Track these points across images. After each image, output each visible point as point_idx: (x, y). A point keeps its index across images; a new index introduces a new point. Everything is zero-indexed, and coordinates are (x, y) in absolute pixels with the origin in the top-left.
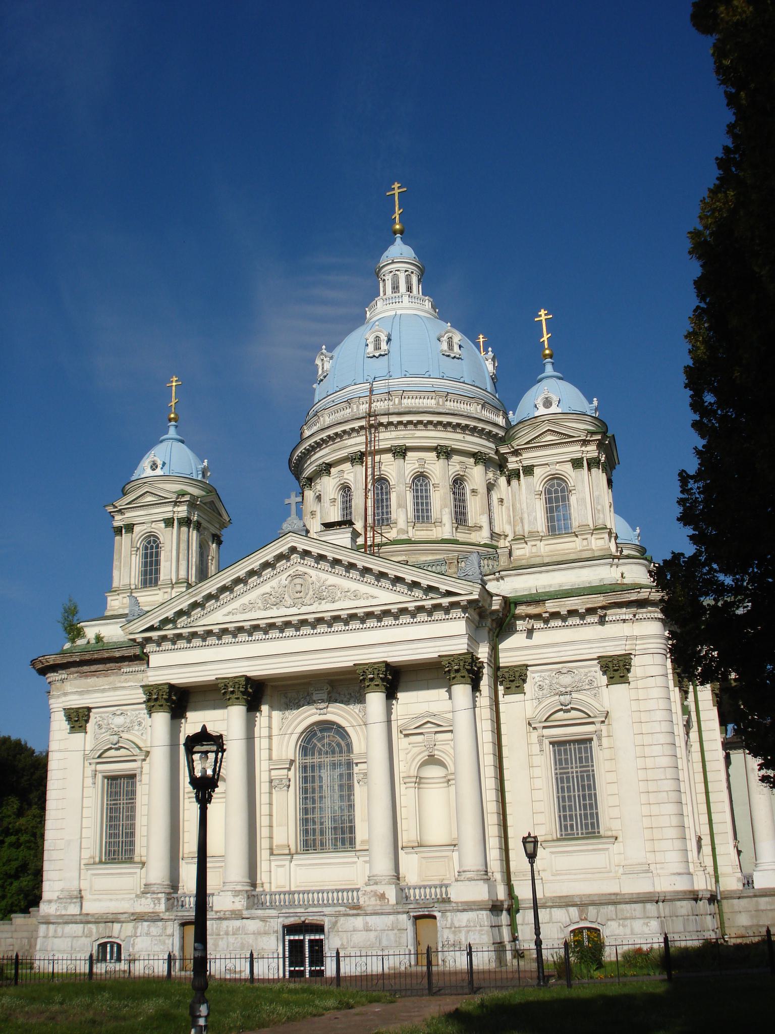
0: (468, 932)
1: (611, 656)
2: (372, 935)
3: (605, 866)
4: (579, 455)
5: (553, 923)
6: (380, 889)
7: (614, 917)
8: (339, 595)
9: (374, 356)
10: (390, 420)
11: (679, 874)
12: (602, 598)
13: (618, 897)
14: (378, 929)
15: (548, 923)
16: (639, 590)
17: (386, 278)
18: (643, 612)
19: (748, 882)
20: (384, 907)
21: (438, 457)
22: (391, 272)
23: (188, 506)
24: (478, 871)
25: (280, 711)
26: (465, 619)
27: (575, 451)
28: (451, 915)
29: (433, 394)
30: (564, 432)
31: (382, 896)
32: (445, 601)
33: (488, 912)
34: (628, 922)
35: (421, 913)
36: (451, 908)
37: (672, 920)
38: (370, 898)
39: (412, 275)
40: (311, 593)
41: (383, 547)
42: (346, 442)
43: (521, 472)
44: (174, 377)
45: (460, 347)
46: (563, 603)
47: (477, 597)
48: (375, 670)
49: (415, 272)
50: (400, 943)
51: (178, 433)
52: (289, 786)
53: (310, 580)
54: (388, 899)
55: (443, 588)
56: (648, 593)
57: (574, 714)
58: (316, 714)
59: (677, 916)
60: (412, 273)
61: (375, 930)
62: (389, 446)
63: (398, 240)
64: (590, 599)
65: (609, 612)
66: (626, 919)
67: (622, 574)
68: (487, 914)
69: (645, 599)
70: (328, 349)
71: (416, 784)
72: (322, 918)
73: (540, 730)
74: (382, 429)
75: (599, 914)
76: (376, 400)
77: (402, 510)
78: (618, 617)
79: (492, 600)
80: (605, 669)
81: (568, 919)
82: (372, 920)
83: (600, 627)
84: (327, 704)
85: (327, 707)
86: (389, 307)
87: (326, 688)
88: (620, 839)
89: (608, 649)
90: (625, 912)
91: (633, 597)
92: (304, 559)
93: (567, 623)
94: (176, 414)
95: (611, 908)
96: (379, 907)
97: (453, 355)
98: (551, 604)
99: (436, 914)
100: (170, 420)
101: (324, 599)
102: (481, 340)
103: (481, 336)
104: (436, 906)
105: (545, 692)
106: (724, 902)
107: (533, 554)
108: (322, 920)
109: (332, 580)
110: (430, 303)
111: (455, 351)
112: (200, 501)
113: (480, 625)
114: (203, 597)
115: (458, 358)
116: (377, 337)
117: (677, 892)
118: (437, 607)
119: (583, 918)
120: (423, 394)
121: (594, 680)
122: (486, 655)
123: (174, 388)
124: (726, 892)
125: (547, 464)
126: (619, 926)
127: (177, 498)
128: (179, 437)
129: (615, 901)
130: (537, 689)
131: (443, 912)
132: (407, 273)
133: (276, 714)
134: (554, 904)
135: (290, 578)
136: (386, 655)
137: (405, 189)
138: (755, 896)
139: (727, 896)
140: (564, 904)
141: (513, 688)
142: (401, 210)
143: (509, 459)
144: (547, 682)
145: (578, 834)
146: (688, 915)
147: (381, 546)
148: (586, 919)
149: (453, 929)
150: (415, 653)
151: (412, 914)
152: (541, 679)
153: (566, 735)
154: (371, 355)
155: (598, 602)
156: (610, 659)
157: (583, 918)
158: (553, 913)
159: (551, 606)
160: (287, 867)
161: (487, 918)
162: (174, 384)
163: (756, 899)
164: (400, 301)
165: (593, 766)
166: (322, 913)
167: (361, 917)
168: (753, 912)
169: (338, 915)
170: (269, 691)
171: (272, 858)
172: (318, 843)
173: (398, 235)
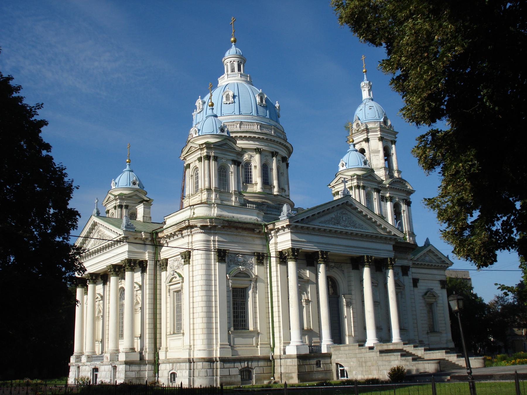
2: (105, 372)
4: (199, 156)
11: (199, 350)
24: (126, 349)
39: (234, 62)
46: (168, 231)
56: (188, 223)
63: (233, 46)
66: (181, 369)
79: (142, 234)
94: (129, 160)
95: (179, 364)
97: (228, 103)
100: (127, 162)
112: (124, 197)
114: (80, 243)
115: (232, 103)
132: (232, 62)
151: (113, 365)
173: (233, 43)
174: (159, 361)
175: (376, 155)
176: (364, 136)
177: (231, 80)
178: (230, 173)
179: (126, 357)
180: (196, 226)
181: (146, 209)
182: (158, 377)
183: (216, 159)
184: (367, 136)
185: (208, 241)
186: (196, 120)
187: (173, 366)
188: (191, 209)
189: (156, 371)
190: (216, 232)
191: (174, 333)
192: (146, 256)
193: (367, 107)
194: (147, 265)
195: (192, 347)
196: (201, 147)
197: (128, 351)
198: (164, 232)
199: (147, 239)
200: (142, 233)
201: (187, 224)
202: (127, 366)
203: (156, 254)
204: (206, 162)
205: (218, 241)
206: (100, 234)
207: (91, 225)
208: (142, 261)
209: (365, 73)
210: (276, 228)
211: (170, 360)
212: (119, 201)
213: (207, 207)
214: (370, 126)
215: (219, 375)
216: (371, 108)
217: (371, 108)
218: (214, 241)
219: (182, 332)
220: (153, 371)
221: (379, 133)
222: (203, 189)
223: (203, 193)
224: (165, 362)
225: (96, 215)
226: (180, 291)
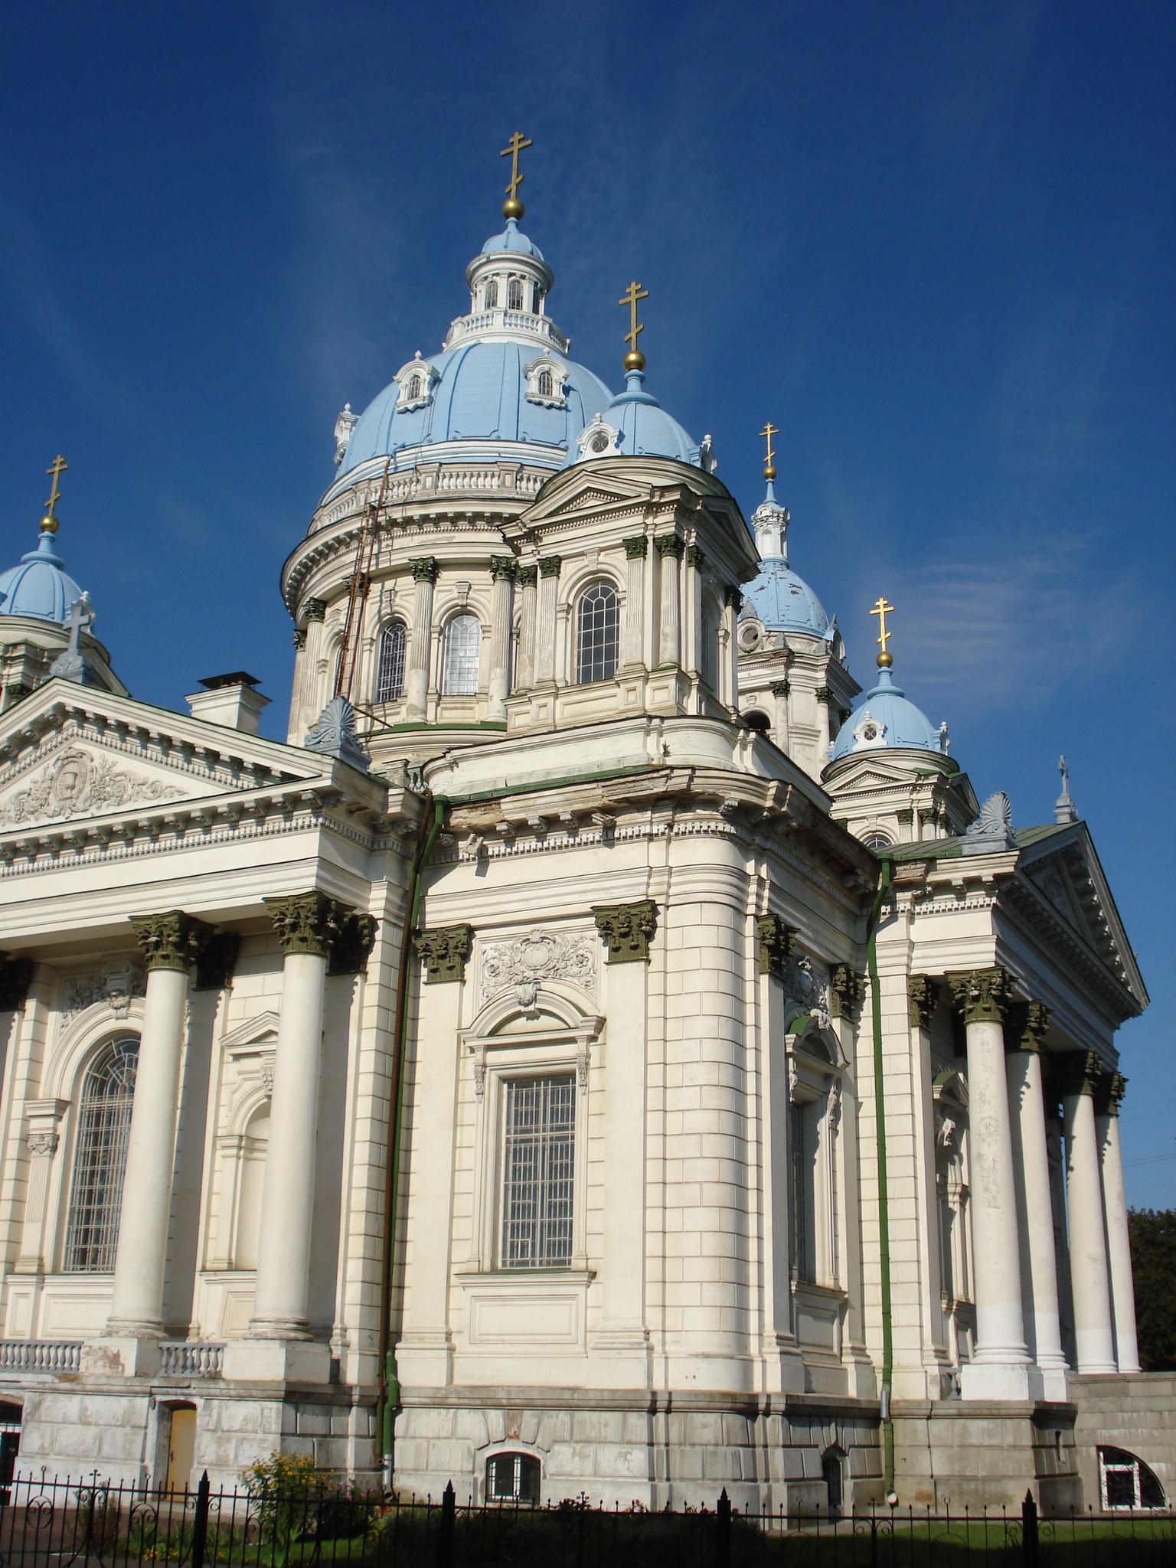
0: (242, 1440)
1: (616, 908)
2: (91, 1432)
3: (567, 1331)
4: (638, 532)
5: (457, 1439)
6: (114, 1345)
7: (567, 1436)
8: (130, 791)
9: (408, 410)
10: (409, 514)
11: (706, 1356)
12: (600, 791)
13: (576, 1396)
14: (101, 1422)
15: (450, 1438)
16: (668, 772)
17: (478, 290)
18: (687, 820)
19: (949, 1385)
20: (112, 1381)
21: (494, 578)
22: (486, 278)
23: (26, 664)
24: (278, 1321)
25: (62, 1010)
26: (319, 828)
27: (631, 524)
28: (220, 1407)
29: (495, 468)
30: (613, 490)
31: (115, 1360)
32: (276, 793)
33: (280, 1405)
34: (590, 1449)
35: (174, 1398)
36: (218, 1392)
37: (682, 1451)
38: (95, 1362)
39: (522, 281)
40: (88, 788)
41: (374, 738)
42: (343, 559)
43: (539, 572)
44: (59, 456)
45: (567, 390)
46: (531, 802)
47: (328, 783)
48: (163, 928)
49: (528, 275)
50: (130, 1454)
51: (53, 551)
52: (54, 1149)
53: (89, 765)
54: (123, 1366)
55: (277, 768)
56: (686, 779)
57: (545, 1021)
58: (109, 1018)
59: (693, 1445)
60: (523, 277)
61: (97, 1425)
62: (406, 561)
63: (512, 227)
64: (579, 794)
65: (620, 820)
66: (588, 1441)
67: (665, 747)
68: (277, 1409)
69: (682, 791)
70: (353, 411)
71: (242, 1153)
72: (21, 1393)
73: (479, 1054)
74: (397, 531)
75: (541, 1428)
76: (395, 483)
77: (416, 673)
78: (636, 830)
79: (386, 797)
80: (606, 930)
81: (484, 1435)
82: (95, 1404)
83: (607, 849)
84: (127, 998)
85: (129, 1004)
86: (470, 334)
87: (124, 969)
88: (599, 1278)
89: (616, 893)
90: (588, 1428)
91: (658, 787)
92: (83, 728)
93: (546, 844)
94: (55, 519)
95: (563, 1416)
96: (104, 1380)
97: (547, 402)
98: (511, 806)
99: (198, 1402)
100: (43, 528)
101: (105, 799)
102: (769, 432)
103: (769, 427)
104: (193, 1386)
105: (499, 978)
106: (898, 1424)
107: (539, 723)
108: (21, 1398)
109: (124, 763)
110: (547, 327)
111: (554, 395)
113: (376, 847)
115: (560, 408)
116: (416, 376)
117: (697, 1394)
118: (266, 807)
119: (512, 1433)
120: (475, 469)
121: (588, 955)
122: (382, 904)
123: (56, 476)
124: (902, 1404)
125: (582, 554)
126: (574, 1454)
127: (6, 652)
128: (53, 557)
129: (571, 1402)
130: (487, 974)
131: (209, 1398)
133: (53, 1017)
134: (462, 1401)
135: (59, 763)
136: (184, 899)
137: (529, 142)
138: (961, 1416)
139: (903, 1412)
140: (478, 1402)
141: (444, 972)
142: (520, 178)
143: (523, 549)
144: (506, 958)
145: (533, 1263)
146: (717, 1445)
147: (371, 736)
148: (517, 1436)
149: (219, 1433)
150: (232, 894)
151: (158, 1398)
152: (495, 954)
153: (526, 1064)
154: (402, 408)
155: (594, 798)
156: (616, 914)
157: (512, 1433)
158: (459, 1419)
159: (511, 810)
160: (32, 1296)
161: (277, 1417)
162: (57, 469)
163: (963, 1421)
164: (490, 322)
165: (573, 1128)
166: (19, 1384)
167: (79, 1397)
168: (955, 1449)
169: (43, 1390)
170: (41, 975)
171: (11, 1279)
172: (90, 1256)
174: (402, 1393)
175: (806, 742)
176: (776, 674)
177: (520, 335)
178: (721, 633)
179: (289, 1365)
180: (711, 802)
181: (247, 715)
182: (393, 1471)
183: (699, 561)
184: (787, 675)
185: (743, 877)
186: (389, 435)
187: (509, 1422)
188: (648, 733)
189: (383, 1440)
190: (768, 845)
191: (494, 1271)
192: (377, 901)
193: (784, 587)
194: (372, 941)
195: (655, 1339)
196: (656, 500)
197: (292, 1335)
198: (503, 806)
199: (397, 821)
200: (391, 791)
201: (679, 782)
202: (287, 1406)
203: (411, 902)
204: (668, 562)
205: (773, 888)
206: (71, 768)
207: (32, 723)
208: (355, 919)
209: (770, 479)
210: (929, 884)
211: (501, 1394)
212: (20, 668)
213: (722, 734)
214: (796, 645)
215: (781, 1474)
216: (794, 589)
217: (794, 589)
218: (761, 882)
219: (577, 1263)
220: (370, 1441)
221: (822, 675)
222: (650, 670)
223: (650, 684)
224: (451, 1401)
225: (79, 679)
226: (563, 1079)
